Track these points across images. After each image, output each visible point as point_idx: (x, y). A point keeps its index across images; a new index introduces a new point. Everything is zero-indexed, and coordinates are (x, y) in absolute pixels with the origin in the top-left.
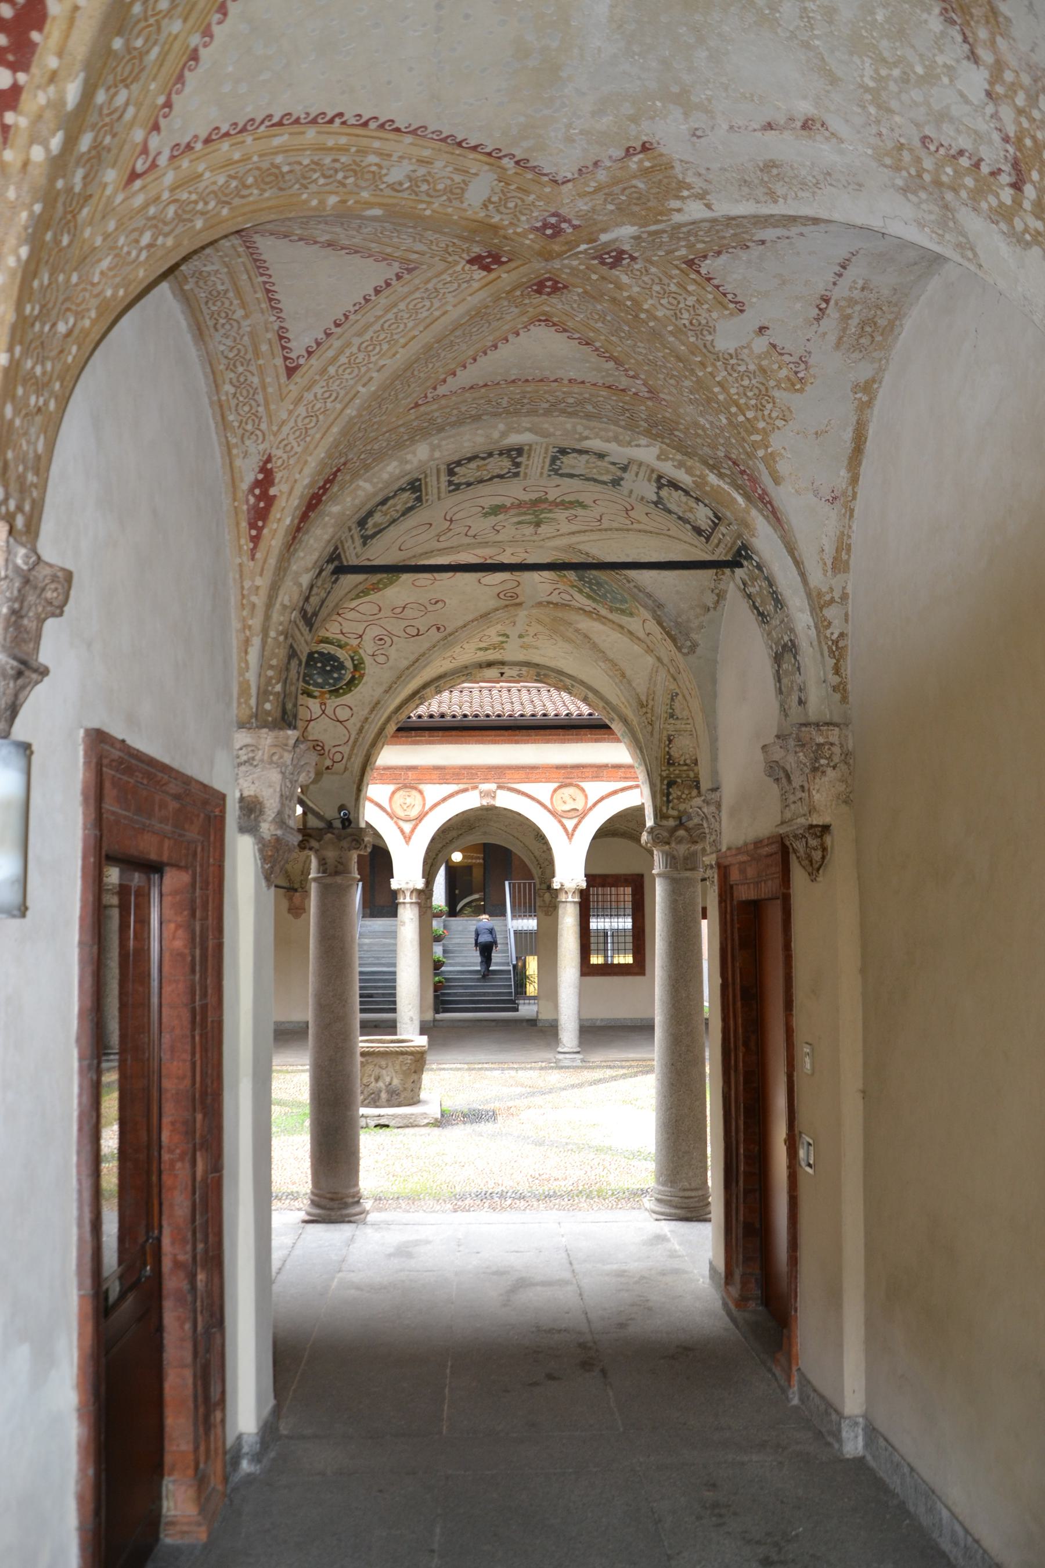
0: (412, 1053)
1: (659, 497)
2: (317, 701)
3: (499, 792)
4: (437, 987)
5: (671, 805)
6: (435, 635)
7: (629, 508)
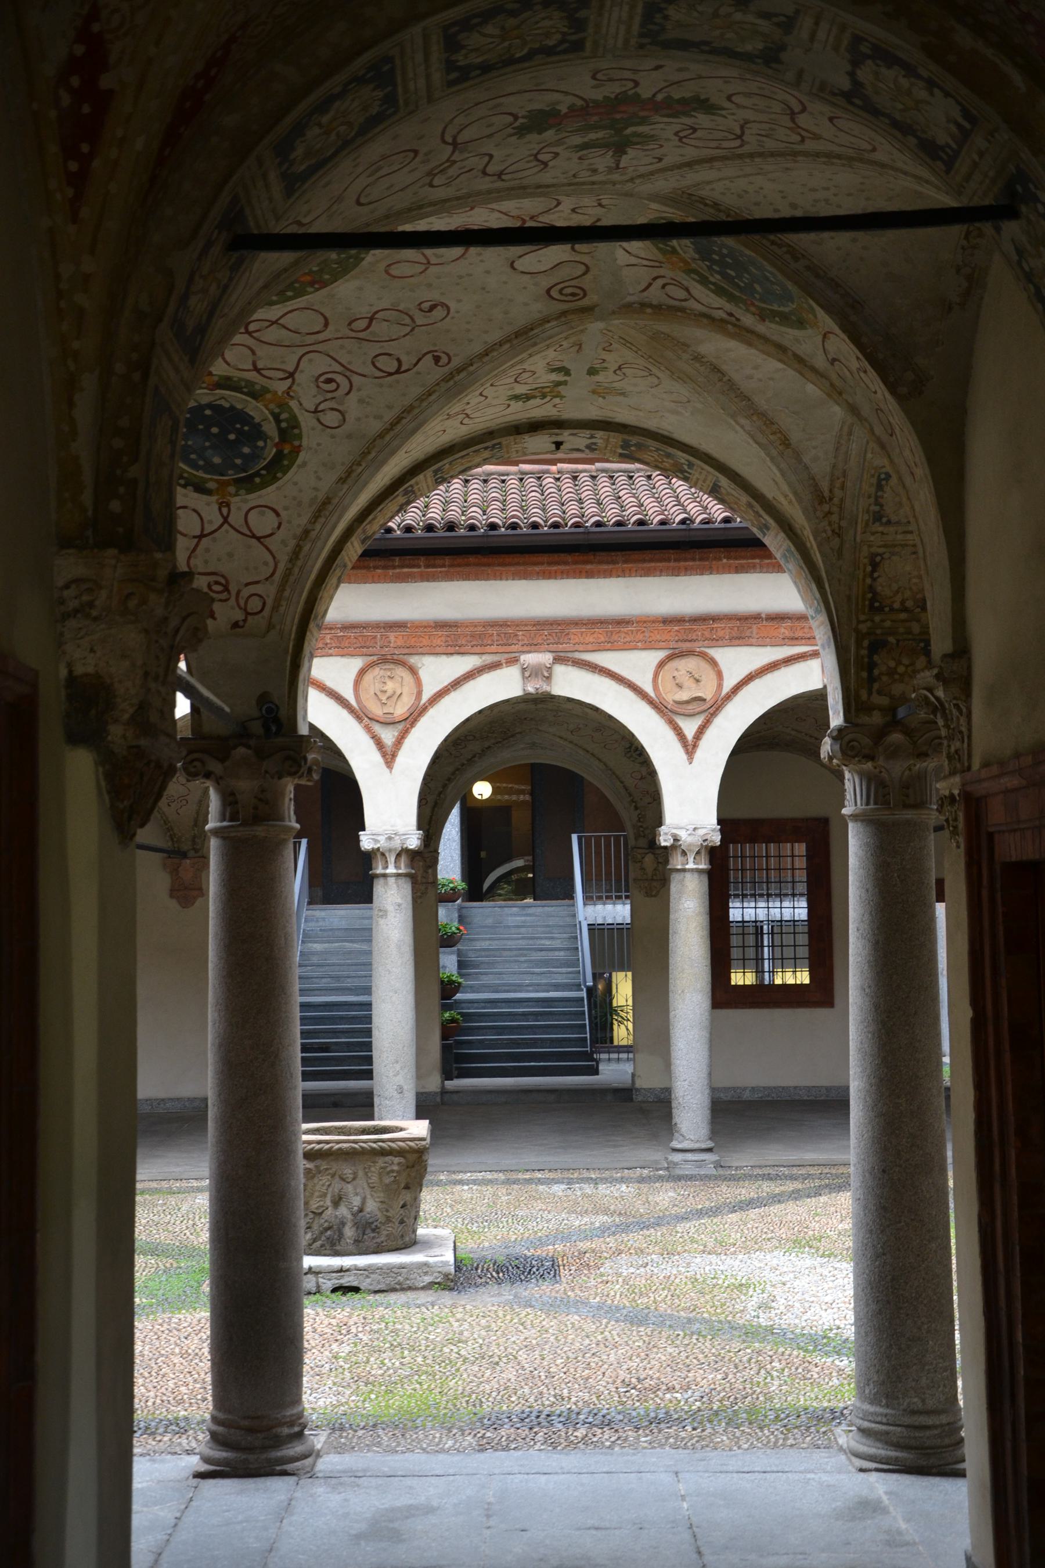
0: (400, 1153)
1: (857, 84)
2: (214, 498)
3: (559, 670)
4: (448, 1031)
5: (876, 686)
6: (430, 373)
7: (797, 108)
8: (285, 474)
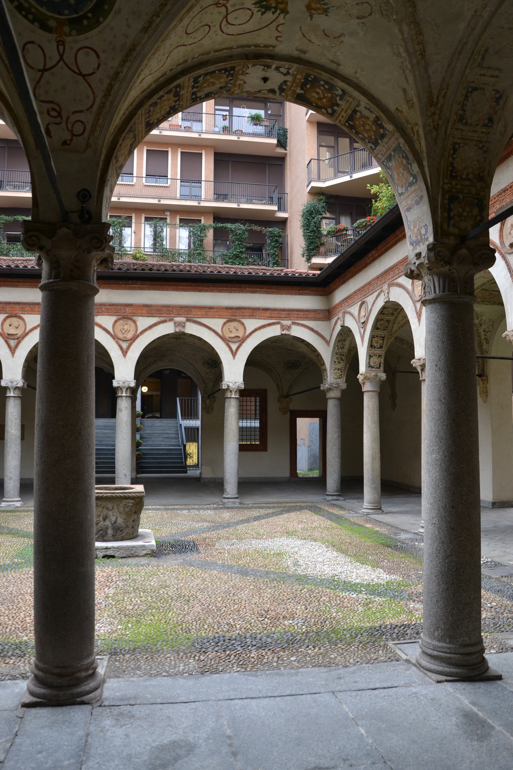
0: (133, 498)
2: (54, 36)
3: (188, 324)
5: (452, 222)
8: (105, 18)
